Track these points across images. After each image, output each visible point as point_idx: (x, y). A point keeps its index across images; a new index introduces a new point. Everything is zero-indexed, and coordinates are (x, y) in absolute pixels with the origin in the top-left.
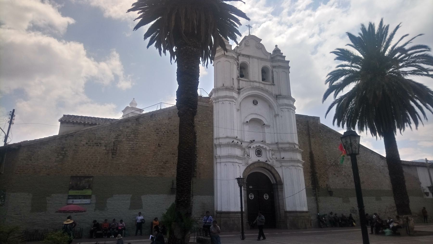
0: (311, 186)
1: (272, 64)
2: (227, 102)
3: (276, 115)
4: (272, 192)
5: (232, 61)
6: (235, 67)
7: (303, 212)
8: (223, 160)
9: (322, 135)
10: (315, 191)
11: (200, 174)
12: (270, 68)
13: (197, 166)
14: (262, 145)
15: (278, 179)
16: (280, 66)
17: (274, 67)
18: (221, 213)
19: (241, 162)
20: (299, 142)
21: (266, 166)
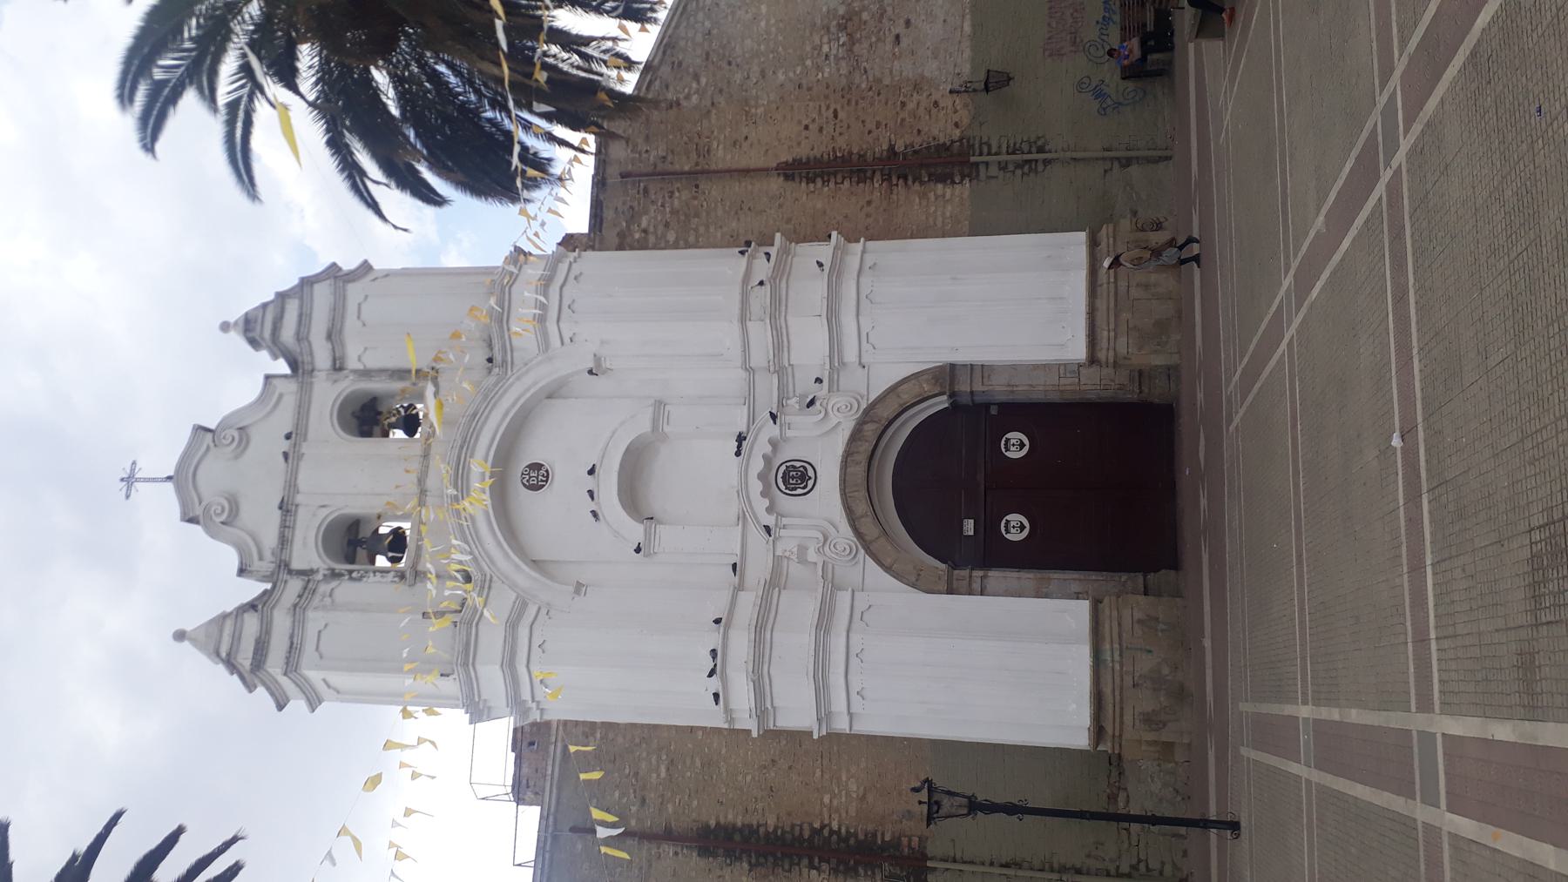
5: (315, 619)
6: (345, 590)
8: (839, 704)
10: (987, 164)
13: (870, 828)
14: (758, 465)
16: (329, 337)
17: (338, 366)
18: (1098, 731)
19: (843, 599)
21: (866, 447)
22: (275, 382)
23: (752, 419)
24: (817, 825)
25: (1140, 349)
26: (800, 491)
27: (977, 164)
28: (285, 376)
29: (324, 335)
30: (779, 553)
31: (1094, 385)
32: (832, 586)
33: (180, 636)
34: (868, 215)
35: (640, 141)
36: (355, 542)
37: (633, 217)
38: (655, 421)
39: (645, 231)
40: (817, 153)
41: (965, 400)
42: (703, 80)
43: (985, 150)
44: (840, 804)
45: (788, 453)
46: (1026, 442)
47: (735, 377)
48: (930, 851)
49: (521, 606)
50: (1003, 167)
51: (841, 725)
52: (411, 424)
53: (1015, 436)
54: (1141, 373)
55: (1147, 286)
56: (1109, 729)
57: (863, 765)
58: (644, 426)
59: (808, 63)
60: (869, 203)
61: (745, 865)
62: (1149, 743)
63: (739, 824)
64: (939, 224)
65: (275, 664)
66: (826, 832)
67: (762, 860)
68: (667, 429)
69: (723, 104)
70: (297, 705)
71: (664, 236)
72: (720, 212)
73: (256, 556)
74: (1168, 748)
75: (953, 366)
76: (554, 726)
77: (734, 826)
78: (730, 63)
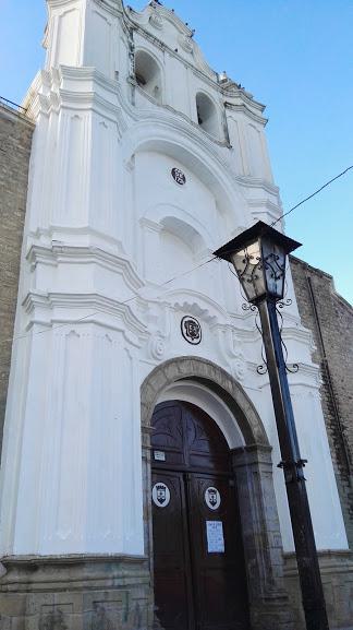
4: (231, 482)
12: (218, 108)
14: (203, 306)
15: (255, 430)
17: (226, 104)
21: (218, 379)
26: (185, 331)
36: (143, 75)
40: (335, 385)
41: (238, 460)
45: (204, 328)
46: (217, 506)
53: (218, 498)
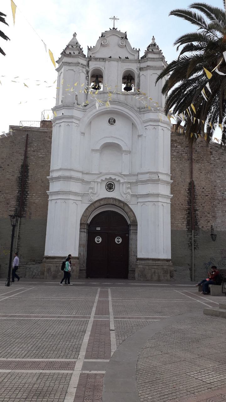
0: (185, 227)
1: (138, 65)
2: (63, 123)
3: (139, 136)
4: (127, 235)
6: (83, 76)
7: (159, 260)
8: (54, 197)
9: (212, 159)
11: (31, 214)
12: (136, 72)
14: (113, 177)
16: (148, 66)
17: (141, 69)
19: (80, 198)
20: (172, 170)
21: (117, 204)
22: (138, 53)
23: (125, 175)
24: (28, 192)
25: (139, 271)
27: (192, 232)
28: (139, 56)
29: (149, 65)
30: (92, 183)
31: (132, 259)
32: (83, 195)
33: (75, 35)
34: (179, 204)
35: (201, 145)
37: (180, 144)
38: (125, 151)
39: (176, 147)
40: (196, 191)
42: (218, 161)
43: (195, 234)
44: (33, 198)
46: (119, 243)
47: (137, 170)
48: (22, 218)
49: (79, 120)
50: (191, 238)
51: (50, 199)
52: (128, 89)
53: (121, 240)
54: (134, 271)
55: (155, 273)
56: (47, 260)
57: (42, 203)
58: (124, 148)
59: (222, 188)
60: (182, 205)
61: (19, 176)
62: (44, 269)
63: (28, 174)
64: (175, 222)
65: (66, 59)
66: (27, 194)
67: (20, 180)
68: (123, 154)
69: (211, 166)
70: (57, 66)
71: (175, 152)
72: (181, 166)
73: (93, 52)
74: (43, 273)
75: (137, 225)
76: (51, 129)
77: (28, 173)
78: (222, 168)
